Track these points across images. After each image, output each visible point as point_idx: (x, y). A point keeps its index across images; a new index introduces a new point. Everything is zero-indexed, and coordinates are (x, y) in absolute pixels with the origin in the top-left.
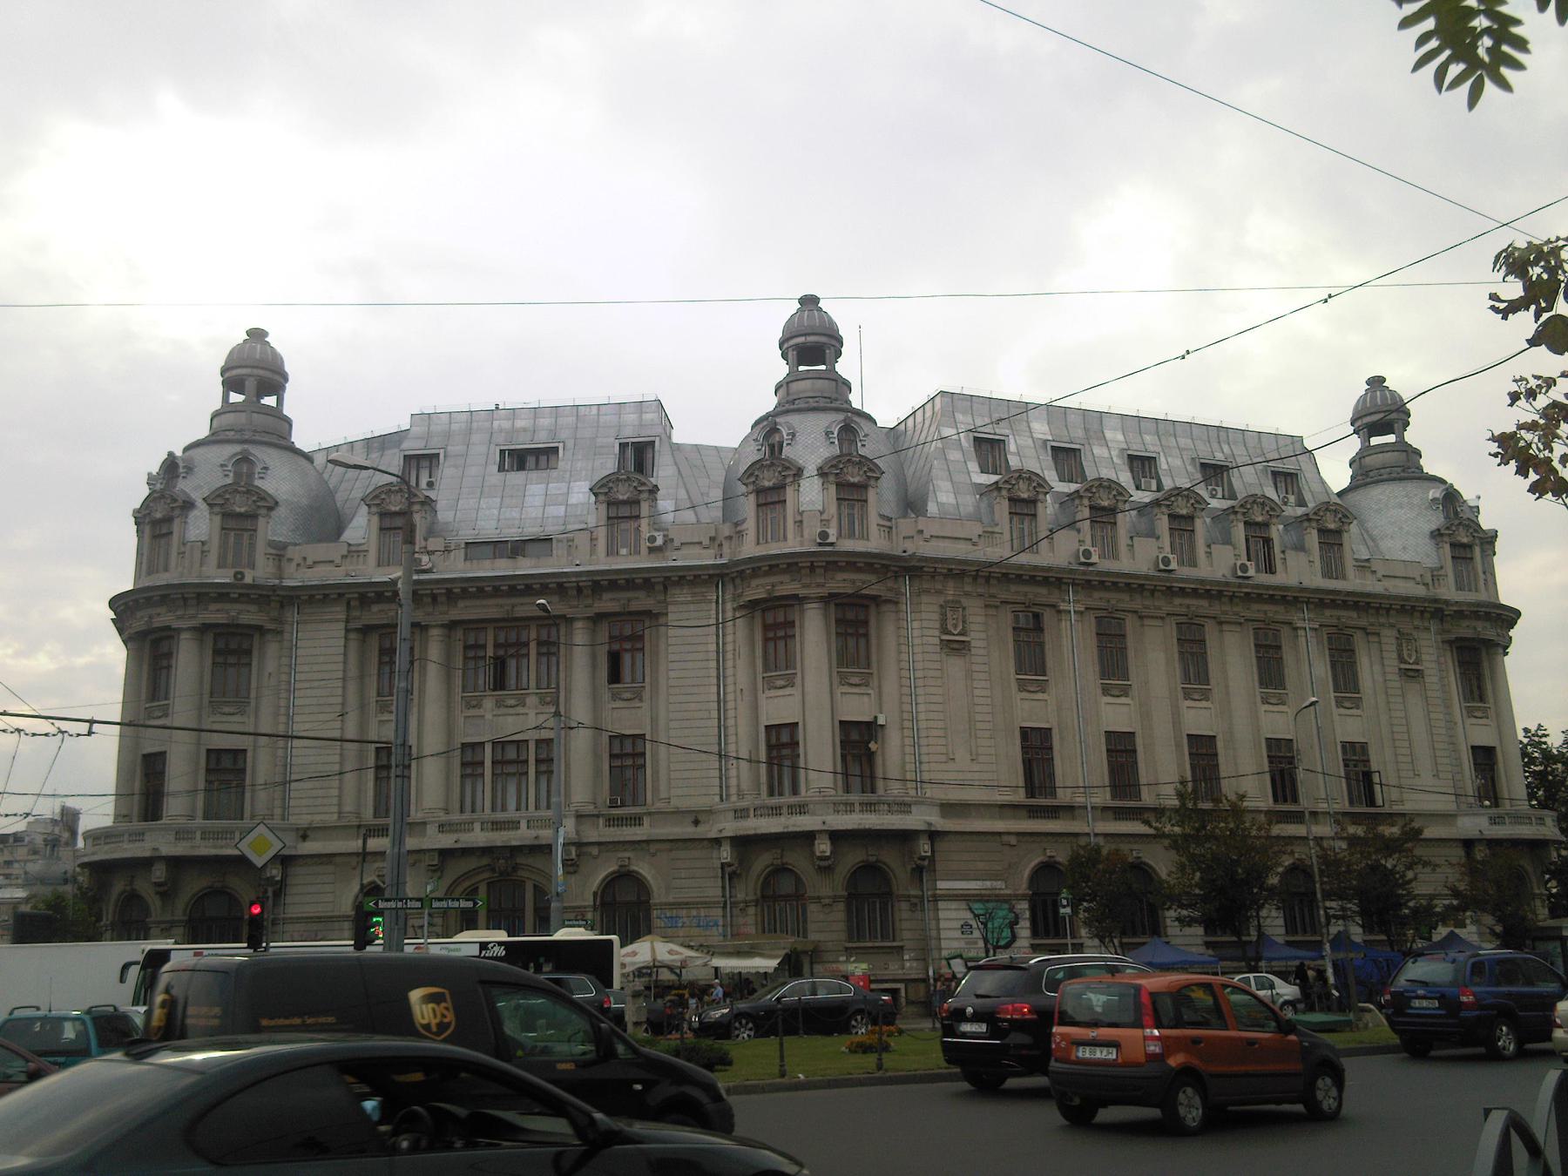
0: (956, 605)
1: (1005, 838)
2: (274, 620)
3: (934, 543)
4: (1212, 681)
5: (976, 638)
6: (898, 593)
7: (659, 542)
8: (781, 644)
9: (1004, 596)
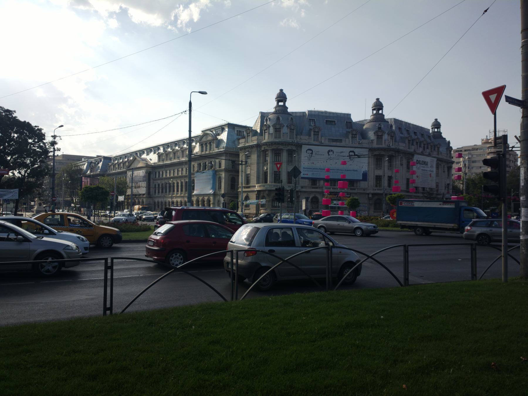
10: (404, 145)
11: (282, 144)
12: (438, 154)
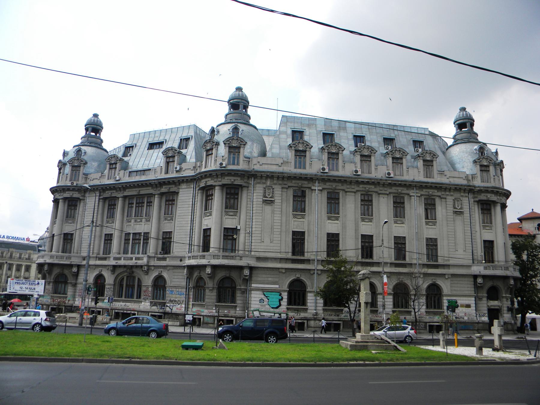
0: (270, 187)
1: (280, 270)
2: (82, 196)
3: (264, 166)
4: (374, 215)
5: (277, 199)
6: (249, 183)
7: (178, 169)
9: (290, 184)
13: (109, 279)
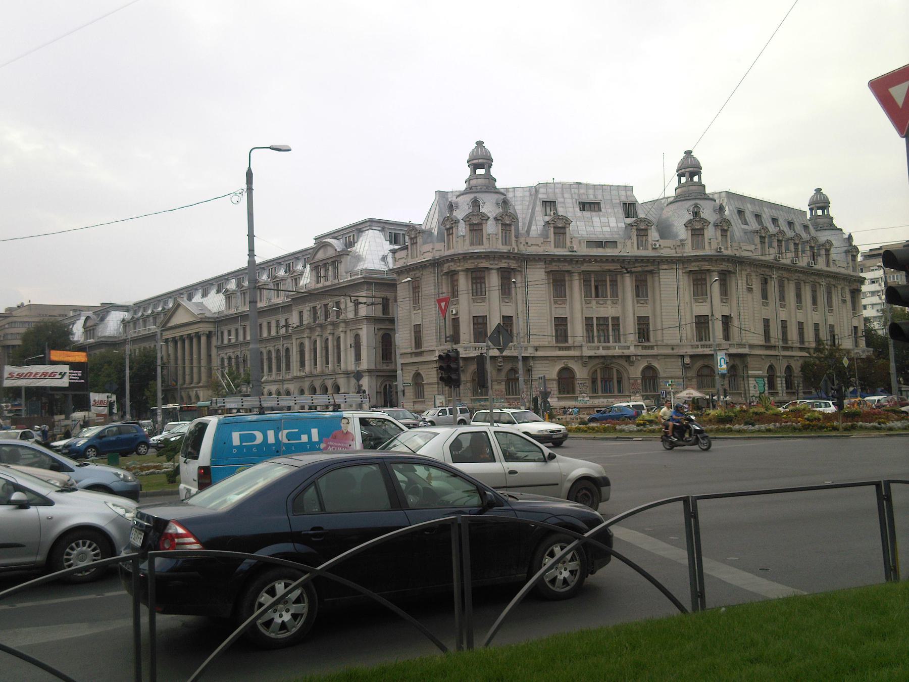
8: (700, 287)
10: (752, 247)
11: (487, 256)
12: (828, 265)
13: (581, 373)
